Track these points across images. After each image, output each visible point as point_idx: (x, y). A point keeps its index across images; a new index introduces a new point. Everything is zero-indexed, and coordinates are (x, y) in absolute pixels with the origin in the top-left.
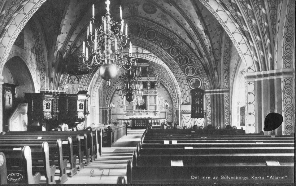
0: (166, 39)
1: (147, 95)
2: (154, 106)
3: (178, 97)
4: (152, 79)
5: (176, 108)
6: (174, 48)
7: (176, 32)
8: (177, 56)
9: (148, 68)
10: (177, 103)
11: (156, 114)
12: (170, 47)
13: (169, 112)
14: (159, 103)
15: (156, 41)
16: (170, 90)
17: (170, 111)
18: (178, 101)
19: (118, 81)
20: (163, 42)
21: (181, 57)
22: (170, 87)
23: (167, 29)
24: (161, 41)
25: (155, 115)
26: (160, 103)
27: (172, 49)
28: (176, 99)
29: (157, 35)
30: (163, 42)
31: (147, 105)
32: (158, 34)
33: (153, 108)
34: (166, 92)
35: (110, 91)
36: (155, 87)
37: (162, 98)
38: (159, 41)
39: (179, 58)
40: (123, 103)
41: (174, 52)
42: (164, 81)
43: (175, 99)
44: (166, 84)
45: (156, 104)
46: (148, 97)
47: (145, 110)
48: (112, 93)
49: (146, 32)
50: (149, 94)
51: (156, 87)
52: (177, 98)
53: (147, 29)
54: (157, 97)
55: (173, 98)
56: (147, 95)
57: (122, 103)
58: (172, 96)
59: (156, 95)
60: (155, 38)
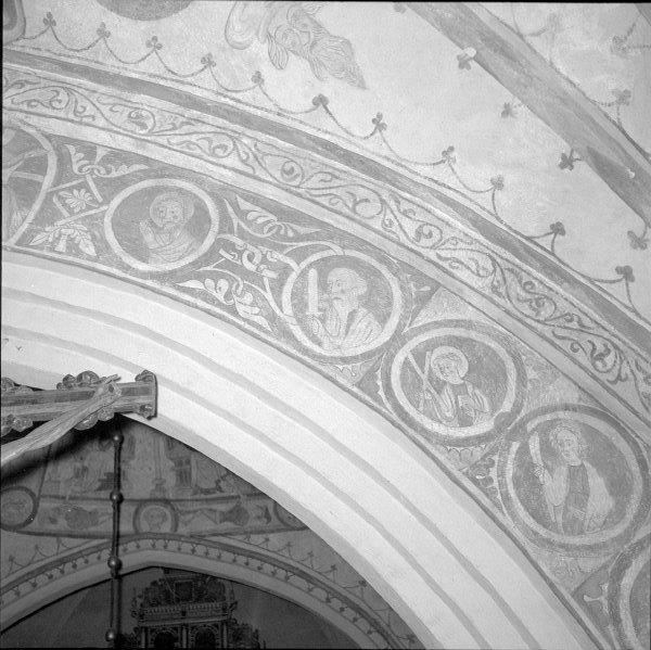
0: (337, 250)
6: (431, 345)
7: (442, 173)
8: (483, 426)
12: (386, 337)
15: (216, 277)
20: (304, 274)
21: (534, 446)
23: (330, 149)
24: (285, 271)
27: (420, 356)
29: (224, 218)
30: (304, 274)
32: (242, 214)
38: (255, 277)
39: (515, 446)
41: (439, 386)
49: (107, 201)
53: (124, 170)
60: (209, 242)
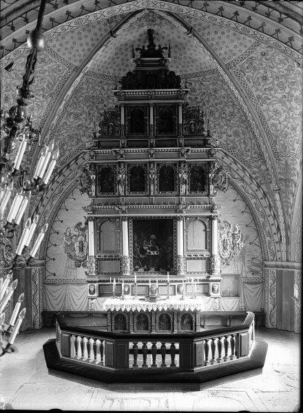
1: (177, 219)
2: (204, 261)
3: (285, 222)
4: (195, 155)
5: (279, 263)
9: (180, 108)
10: (284, 247)
11: (211, 293)
13: (250, 275)
14: (221, 247)
16: (256, 197)
17: (254, 272)
18: (287, 237)
19: (68, 166)
22: (259, 186)
25: (207, 294)
26: (225, 248)
28: (278, 229)
31: (177, 257)
33: (200, 266)
34: (241, 205)
35: (42, 200)
36: (206, 187)
37: (235, 229)
40: (85, 249)
42: (233, 166)
43: (274, 230)
44: (242, 174)
45: (210, 250)
46: (180, 224)
47: (168, 278)
48: (48, 208)
50: (184, 214)
51: (212, 187)
52: (282, 226)
54: (215, 223)
55: (268, 228)
56: (177, 219)
57: (81, 249)
58: (261, 219)
59: (211, 219)
